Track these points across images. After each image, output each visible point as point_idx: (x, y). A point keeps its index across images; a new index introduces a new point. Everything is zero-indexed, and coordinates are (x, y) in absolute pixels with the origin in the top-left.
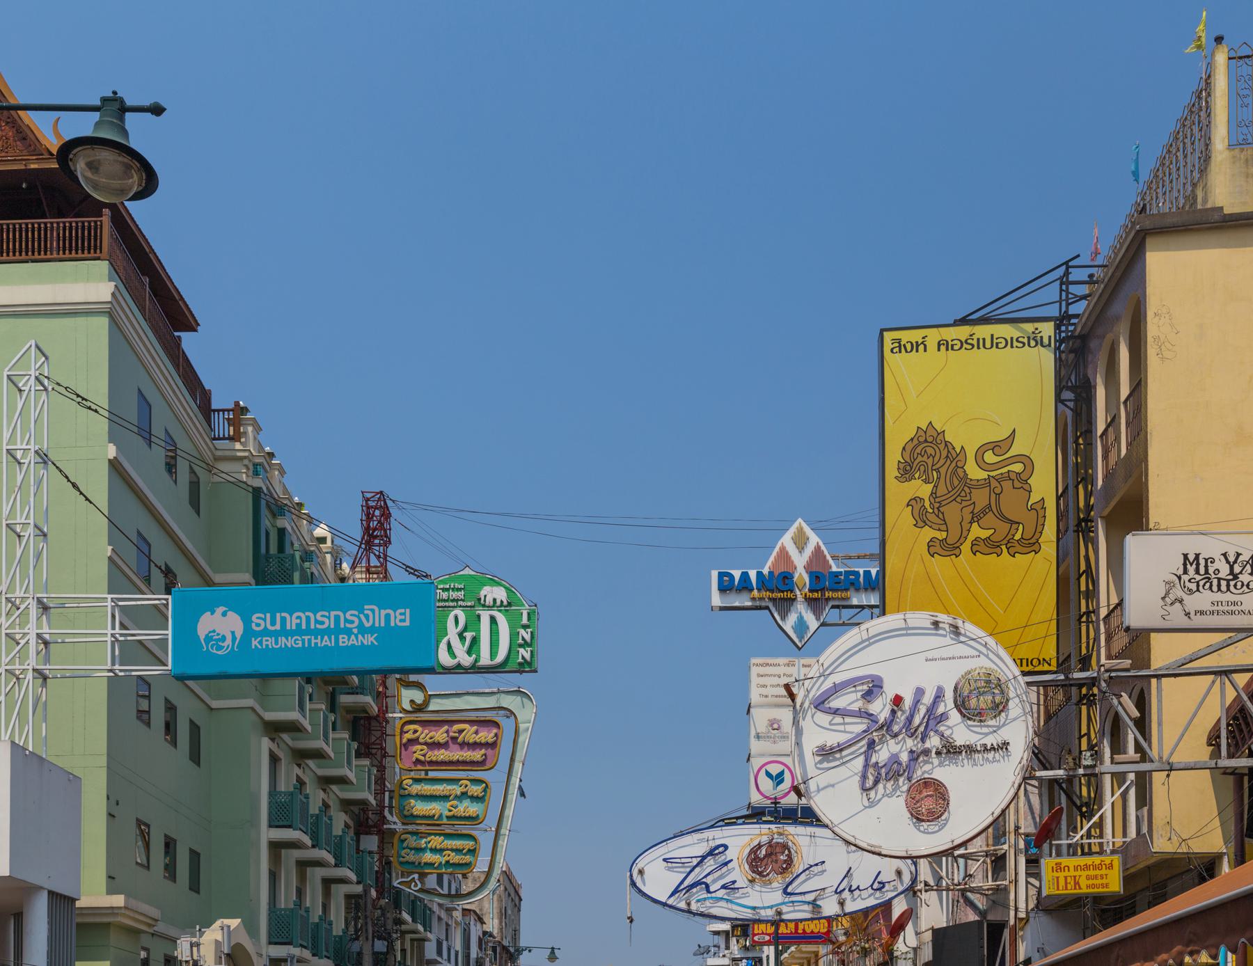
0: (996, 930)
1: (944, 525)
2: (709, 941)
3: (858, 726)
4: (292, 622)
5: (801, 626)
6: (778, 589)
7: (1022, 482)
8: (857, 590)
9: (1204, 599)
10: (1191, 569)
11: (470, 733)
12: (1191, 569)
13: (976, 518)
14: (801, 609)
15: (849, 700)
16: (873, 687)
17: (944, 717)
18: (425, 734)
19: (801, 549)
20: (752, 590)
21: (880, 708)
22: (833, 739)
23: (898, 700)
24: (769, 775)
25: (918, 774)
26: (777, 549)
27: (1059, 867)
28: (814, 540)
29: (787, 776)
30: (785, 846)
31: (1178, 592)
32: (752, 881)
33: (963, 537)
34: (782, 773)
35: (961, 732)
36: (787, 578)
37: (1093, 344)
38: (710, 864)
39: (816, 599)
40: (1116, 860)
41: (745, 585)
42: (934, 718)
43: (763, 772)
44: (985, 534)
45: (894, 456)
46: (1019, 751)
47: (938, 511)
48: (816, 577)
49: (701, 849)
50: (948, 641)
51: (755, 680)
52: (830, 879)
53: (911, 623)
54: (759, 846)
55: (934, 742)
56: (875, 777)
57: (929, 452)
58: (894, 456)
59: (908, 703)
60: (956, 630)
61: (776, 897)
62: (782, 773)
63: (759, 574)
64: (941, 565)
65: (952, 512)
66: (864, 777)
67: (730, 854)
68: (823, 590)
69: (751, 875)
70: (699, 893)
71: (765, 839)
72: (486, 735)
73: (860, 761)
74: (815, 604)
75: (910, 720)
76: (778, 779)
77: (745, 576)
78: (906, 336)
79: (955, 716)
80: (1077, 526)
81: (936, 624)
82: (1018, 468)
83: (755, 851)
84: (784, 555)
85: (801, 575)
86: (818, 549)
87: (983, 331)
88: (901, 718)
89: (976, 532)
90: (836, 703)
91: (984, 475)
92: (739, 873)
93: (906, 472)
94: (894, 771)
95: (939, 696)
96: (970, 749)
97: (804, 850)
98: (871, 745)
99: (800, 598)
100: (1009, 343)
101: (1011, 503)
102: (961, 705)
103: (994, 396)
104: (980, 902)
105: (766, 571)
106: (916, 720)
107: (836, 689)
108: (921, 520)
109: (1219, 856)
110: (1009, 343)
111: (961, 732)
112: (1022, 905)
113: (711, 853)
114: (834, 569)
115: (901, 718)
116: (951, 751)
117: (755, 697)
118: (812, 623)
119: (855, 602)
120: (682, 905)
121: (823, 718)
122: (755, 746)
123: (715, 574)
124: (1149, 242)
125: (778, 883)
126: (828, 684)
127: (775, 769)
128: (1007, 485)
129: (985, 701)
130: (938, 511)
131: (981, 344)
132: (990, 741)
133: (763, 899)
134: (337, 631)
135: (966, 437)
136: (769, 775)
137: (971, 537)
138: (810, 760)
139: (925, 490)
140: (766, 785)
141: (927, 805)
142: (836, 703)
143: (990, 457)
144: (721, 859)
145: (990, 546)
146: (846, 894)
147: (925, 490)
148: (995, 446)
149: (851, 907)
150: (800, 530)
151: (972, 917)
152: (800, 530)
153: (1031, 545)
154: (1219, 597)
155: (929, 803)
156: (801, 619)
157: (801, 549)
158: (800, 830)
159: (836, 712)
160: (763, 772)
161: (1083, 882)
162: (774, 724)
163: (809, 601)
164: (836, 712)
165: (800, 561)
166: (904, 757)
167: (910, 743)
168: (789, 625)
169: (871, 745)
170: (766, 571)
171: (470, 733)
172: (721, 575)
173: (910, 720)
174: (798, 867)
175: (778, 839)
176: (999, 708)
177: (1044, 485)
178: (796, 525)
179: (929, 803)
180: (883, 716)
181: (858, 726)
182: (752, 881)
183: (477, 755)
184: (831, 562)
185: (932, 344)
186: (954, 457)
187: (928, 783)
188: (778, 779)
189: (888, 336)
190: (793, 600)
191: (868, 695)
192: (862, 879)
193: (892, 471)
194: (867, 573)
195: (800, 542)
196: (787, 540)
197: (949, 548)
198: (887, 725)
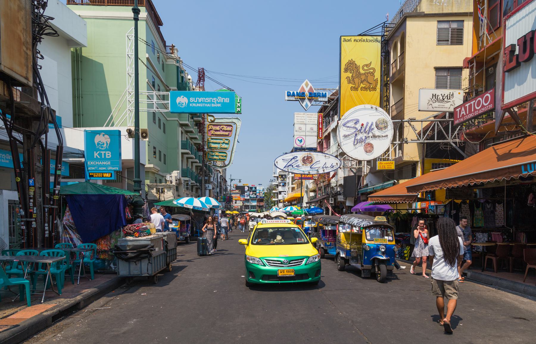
0: (359, 177)
2: (273, 178)
3: (354, 130)
4: (200, 100)
6: (301, 96)
7: (373, 74)
9: (437, 104)
10: (434, 97)
11: (225, 128)
12: (434, 97)
13: (362, 82)
14: (306, 101)
15: (351, 124)
16: (357, 122)
17: (373, 129)
18: (214, 128)
19: (307, 87)
21: (358, 126)
22: (347, 133)
23: (362, 125)
25: (367, 142)
27: (381, 163)
28: (310, 85)
29: (303, 140)
30: (311, 157)
31: (431, 103)
33: (359, 86)
35: (377, 132)
36: (303, 93)
37: (390, 42)
38: (293, 161)
40: (394, 162)
41: (293, 95)
42: (371, 129)
44: (364, 86)
45: (343, 67)
46: (390, 137)
47: (353, 80)
48: (310, 94)
49: (292, 157)
50: (375, 111)
51: (296, 118)
52: (321, 165)
53: (366, 107)
55: (371, 135)
56: (357, 142)
57: (351, 66)
58: (343, 67)
59: (365, 126)
61: (309, 169)
63: (297, 92)
64: (353, 93)
65: (356, 80)
66: (354, 142)
67: (298, 159)
70: (291, 167)
71: (306, 155)
72: (229, 129)
73: (354, 138)
74: (310, 100)
75: (365, 129)
77: (293, 93)
78: (347, 38)
79: (376, 129)
80: (385, 85)
81: (372, 107)
82: (372, 71)
84: (303, 88)
85: (307, 93)
86: (311, 88)
87: (365, 38)
88: (363, 129)
89: (362, 85)
90: (348, 125)
91: (364, 72)
92: (300, 163)
93: (346, 70)
94: (361, 141)
95: (372, 124)
96: (379, 136)
97: (315, 158)
98: (356, 135)
100: (371, 41)
101: (370, 79)
102: (377, 127)
103: (367, 53)
104: (354, 170)
106: (365, 129)
107: (348, 122)
108: (349, 82)
109: (417, 162)
110: (371, 41)
111: (377, 132)
112: (365, 171)
113: (293, 158)
115: (363, 129)
116: (374, 136)
117: (296, 122)
118: (309, 104)
120: (287, 170)
121: (345, 128)
122: (296, 133)
123: (286, 92)
124: (407, 19)
125: (309, 165)
126: (346, 120)
127: (300, 139)
128: (369, 74)
129: (383, 126)
130: (353, 80)
131: (364, 41)
132: (384, 135)
133: (305, 169)
134: (211, 103)
135: (360, 63)
139: (350, 75)
140: (298, 142)
141: (369, 149)
142: (348, 125)
143: (365, 68)
144: (296, 160)
145: (365, 89)
147: (350, 75)
148: (367, 65)
149: (326, 171)
151: (353, 174)
153: (374, 89)
154: (440, 104)
155: (369, 148)
156: (307, 104)
157: (307, 87)
158: (315, 153)
159: (348, 127)
161: (386, 167)
163: (309, 99)
164: (348, 127)
165: (307, 90)
166: (364, 138)
167: (365, 135)
168: (304, 105)
169: (356, 135)
171: (225, 128)
172: (288, 92)
173: (365, 129)
174: (314, 162)
175: (309, 155)
176: (386, 127)
177: (378, 75)
179: (369, 148)
180: (359, 128)
181: (354, 130)
183: (227, 133)
185: (353, 40)
186: (357, 68)
187: (369, 144)
188: (301, 141)
189: (342, 38)
191: (356, 123)
192: (329, 165)
193: (342, 70)
196: (303, 85)
197: (355, 89)
198: (360, 130)
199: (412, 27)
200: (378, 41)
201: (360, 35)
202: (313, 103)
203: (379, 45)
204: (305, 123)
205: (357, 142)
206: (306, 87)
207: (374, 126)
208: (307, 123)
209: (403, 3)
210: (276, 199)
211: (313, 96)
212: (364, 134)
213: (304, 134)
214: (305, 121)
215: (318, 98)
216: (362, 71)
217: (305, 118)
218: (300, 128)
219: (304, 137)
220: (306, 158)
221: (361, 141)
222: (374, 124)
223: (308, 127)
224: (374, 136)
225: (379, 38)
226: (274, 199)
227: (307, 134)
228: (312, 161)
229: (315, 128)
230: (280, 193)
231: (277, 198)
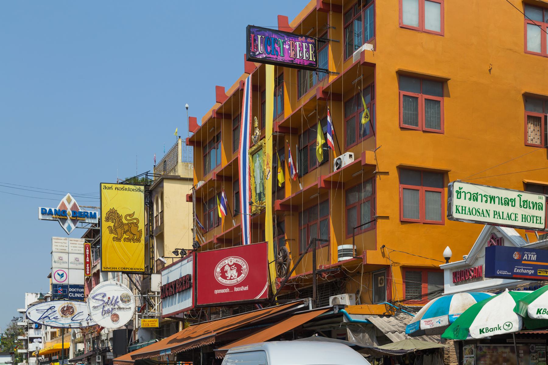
1: (117, 234)
5: (69, 228)
6: (61, 215)
8: (88, 218)
13: (125, 232)
14: (69, 222)
17: (118, 302)
19: (69, 203)
20: (52, 215)
23: (109, 298)
24: (58, 274)
25: (113, 313)
26: (61, 202)
28: (73, 201)
29: (65, 275)
30: (72, 307)
32: (62, 316)
33: (121, 237)
34: (63, 274)
35: (121, 305)
39: (74, 220)
42: (116, 302)
43: (56, 273)
44: (127, 237)
47: (115, 230)
48: (74, 213)
50: (119, 287)
54: (64, 307)
55: (116, 307)
56: (104, 313)
59: (111, 299)
60: (121, 285)
62: (63, 274)
63: (55, 210)
64: (116, 243)
65: (119, 230)
68: (76, 217)
69: (62, 315)
71: (66, 305)
74: (74, 221)
75: (112, 302)
76: (62, 276)
77: (50, 210)
79: (120, 302)
83: (63, 308)
84: (63, 204)
85: (69, 211)
86: (75, 204)
88: (110, 301)
89: (125, 236)
92: (59, 314)
94: (108, 312)
95: (117, 298)
98: (104, 306)
99: (69, 219)
102: (122, 300)
105: (57, 209)
106: (112, 302)
108: (111, 232)
114: (80, 210)
115: (110, 301)
118: (72, 225)
119: (87, 221)
122: (54, 265)
127: (61, 273)
130: (115, 230)
135: (122, 212)
136: (58, 274)
137: (124, 237)
138: (91, 309)
139: (112, 225)
140: (58, 277)
146: (89, 321)
147: (112, 225)
150: (69, 197)
152: (69, 197)
156: (69, 225)
157: (69, 203)
158: (76, 303)
160: (56, 273)
162: (60, 258)
163: (72, 220)
165: (69, 207)
166: (110, 309)
167: (112, 307)
168: (65, 226)
169: (104, 306)
170: (57, 209)
173: (112, 302)
175: (70, 305)
178: (67, 195)
180: (106, 301)
182: (62, 316)
184: (79, 208)
186: (119, 217)
190: (66, 219)
194: (91, 213)
195: (69, 201)
196: (64, 200)
197: (118, 239)
198: (107, 303)
199: (168, 187)
200: (141, 191)
201: (122, 183)
202: (79, 224)
203: (142, 195)
204: (67, 251)
205: (104, 313)
206: (68, 202)
207: (119, 300)
208: (70, 251)
209: (167, 151)
210: (25, 351)
211: (77, 216)
212: (110, 307)
213: (66, 266)
214: (67, 248)
215: (86, 219)
216: (125, 221)
217: (67, 245)
218: (60, 258)
219: (66, 271)
220: (65, 309)
221: (108, 312)
222: (119, 298)
223: (72, 257)
224: (120, 308)
225: (142, 188)
226: (20, 351)
227: (71, 266)
229: (82, 258)
230: (31, 340)
231: (27, 348)
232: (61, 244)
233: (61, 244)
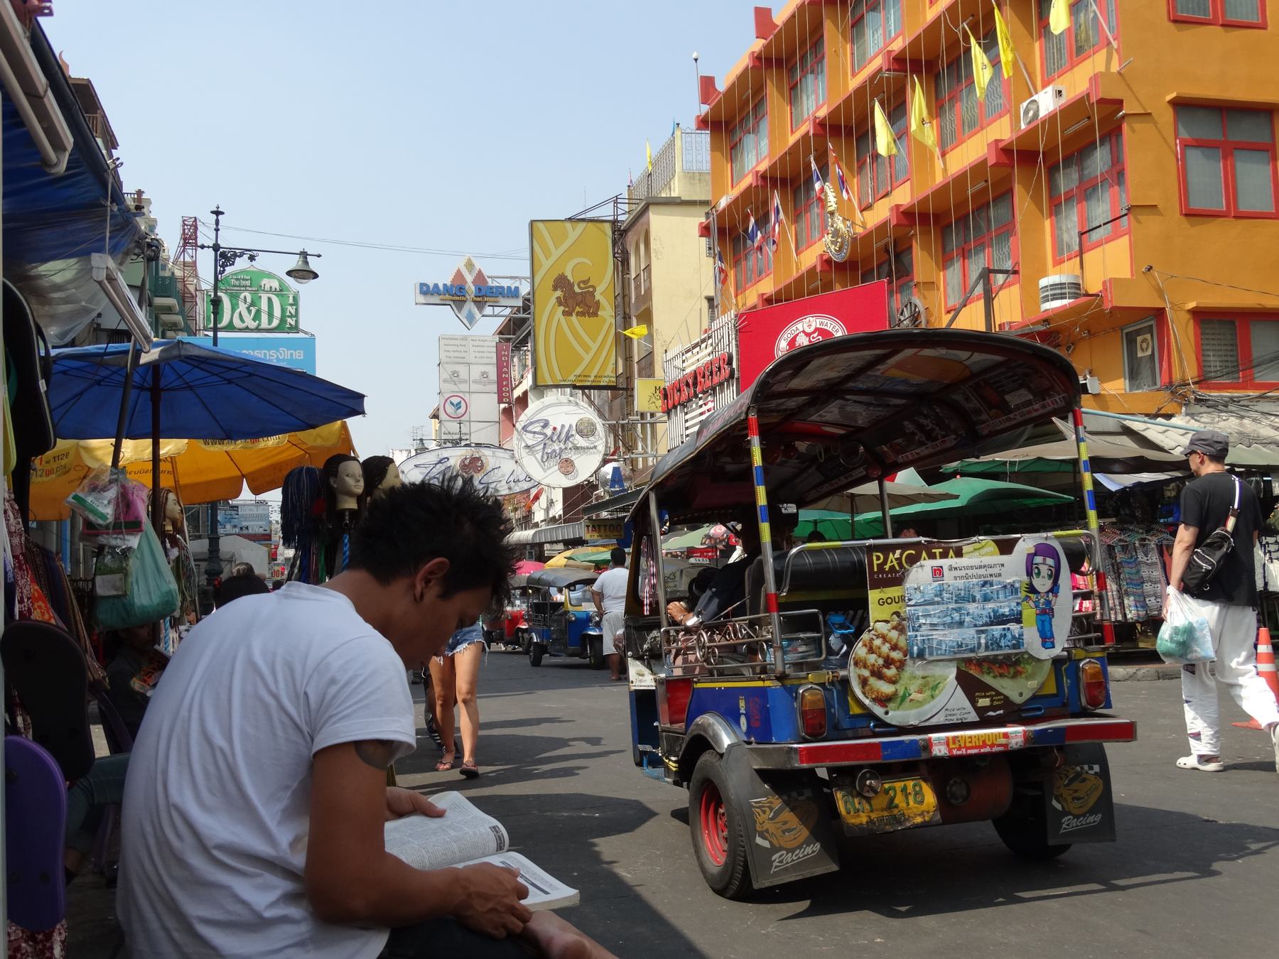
14: (470, 306)
16: (546, 425)
19: (470, 272)
21: (549, 431)
29: (463, 404)
35: (580, 441)
49: (436, 460)
59: (559, 429)
76: (458, 406)
79: (577, 437)
85: (471, 288)
90: (530, 428)
113: (440, 462)
142: (530, 428)
146: (512, 484)
156: (470, 312)
208: (472, 360)
219: (466, 397)
220: (467, 462)
223: (476, 372)
227: (474, 387)
228: (482, 466)
232: (455, 348)
233: (455, 348)
